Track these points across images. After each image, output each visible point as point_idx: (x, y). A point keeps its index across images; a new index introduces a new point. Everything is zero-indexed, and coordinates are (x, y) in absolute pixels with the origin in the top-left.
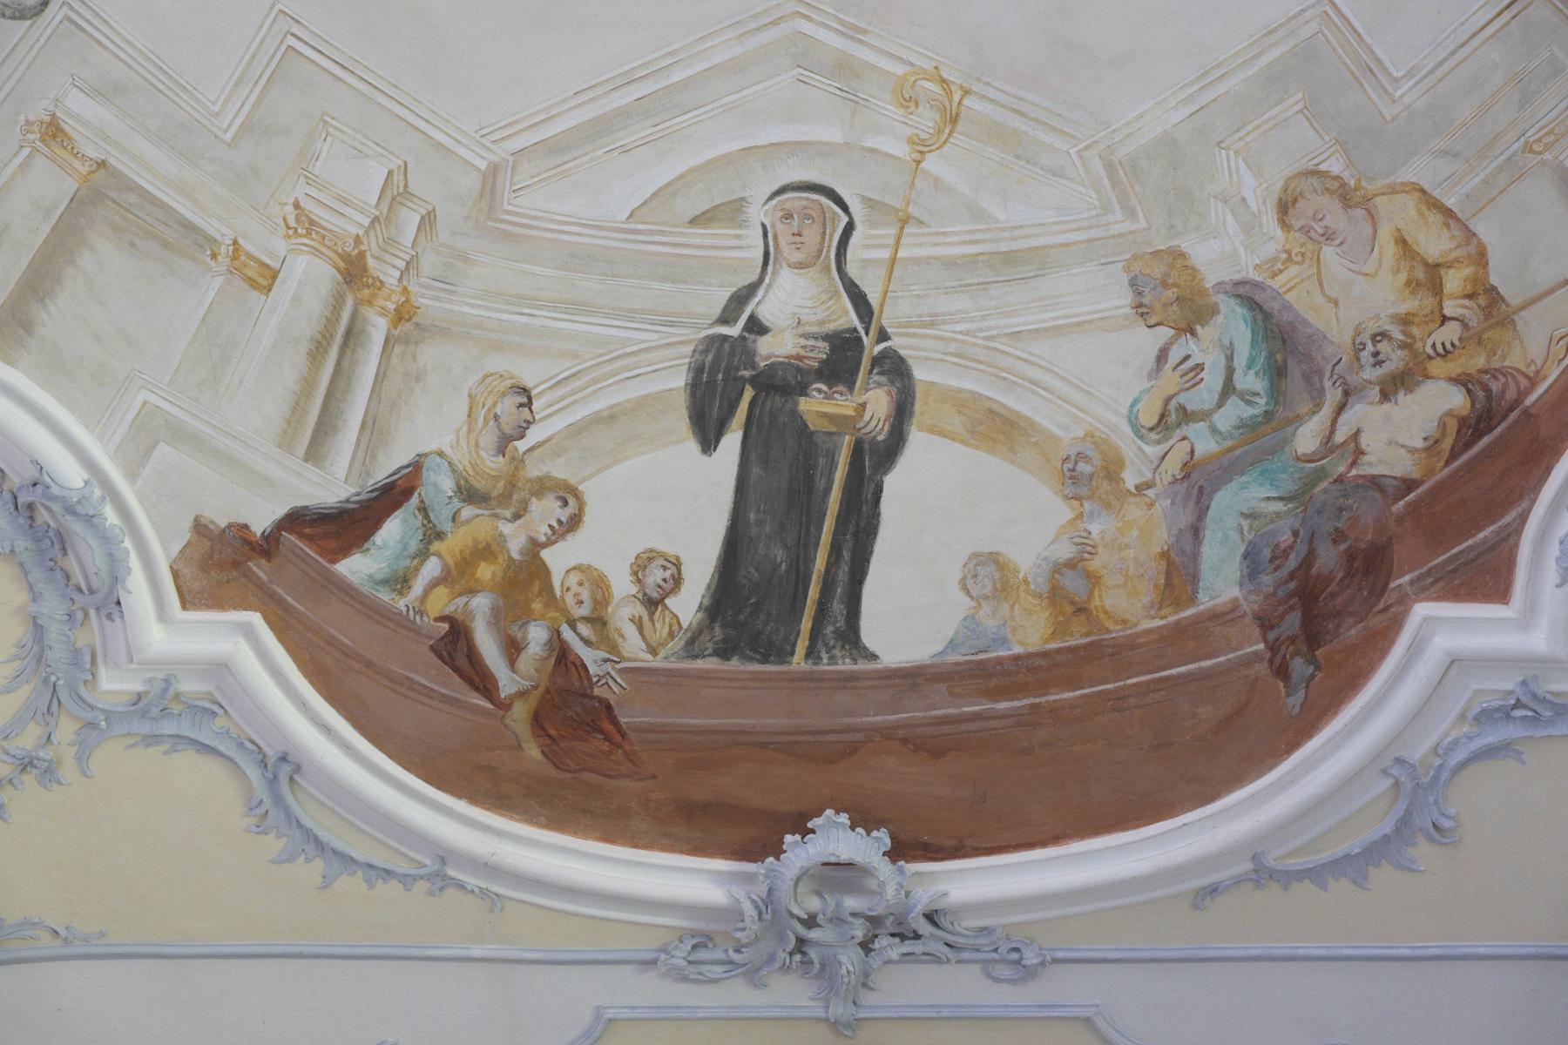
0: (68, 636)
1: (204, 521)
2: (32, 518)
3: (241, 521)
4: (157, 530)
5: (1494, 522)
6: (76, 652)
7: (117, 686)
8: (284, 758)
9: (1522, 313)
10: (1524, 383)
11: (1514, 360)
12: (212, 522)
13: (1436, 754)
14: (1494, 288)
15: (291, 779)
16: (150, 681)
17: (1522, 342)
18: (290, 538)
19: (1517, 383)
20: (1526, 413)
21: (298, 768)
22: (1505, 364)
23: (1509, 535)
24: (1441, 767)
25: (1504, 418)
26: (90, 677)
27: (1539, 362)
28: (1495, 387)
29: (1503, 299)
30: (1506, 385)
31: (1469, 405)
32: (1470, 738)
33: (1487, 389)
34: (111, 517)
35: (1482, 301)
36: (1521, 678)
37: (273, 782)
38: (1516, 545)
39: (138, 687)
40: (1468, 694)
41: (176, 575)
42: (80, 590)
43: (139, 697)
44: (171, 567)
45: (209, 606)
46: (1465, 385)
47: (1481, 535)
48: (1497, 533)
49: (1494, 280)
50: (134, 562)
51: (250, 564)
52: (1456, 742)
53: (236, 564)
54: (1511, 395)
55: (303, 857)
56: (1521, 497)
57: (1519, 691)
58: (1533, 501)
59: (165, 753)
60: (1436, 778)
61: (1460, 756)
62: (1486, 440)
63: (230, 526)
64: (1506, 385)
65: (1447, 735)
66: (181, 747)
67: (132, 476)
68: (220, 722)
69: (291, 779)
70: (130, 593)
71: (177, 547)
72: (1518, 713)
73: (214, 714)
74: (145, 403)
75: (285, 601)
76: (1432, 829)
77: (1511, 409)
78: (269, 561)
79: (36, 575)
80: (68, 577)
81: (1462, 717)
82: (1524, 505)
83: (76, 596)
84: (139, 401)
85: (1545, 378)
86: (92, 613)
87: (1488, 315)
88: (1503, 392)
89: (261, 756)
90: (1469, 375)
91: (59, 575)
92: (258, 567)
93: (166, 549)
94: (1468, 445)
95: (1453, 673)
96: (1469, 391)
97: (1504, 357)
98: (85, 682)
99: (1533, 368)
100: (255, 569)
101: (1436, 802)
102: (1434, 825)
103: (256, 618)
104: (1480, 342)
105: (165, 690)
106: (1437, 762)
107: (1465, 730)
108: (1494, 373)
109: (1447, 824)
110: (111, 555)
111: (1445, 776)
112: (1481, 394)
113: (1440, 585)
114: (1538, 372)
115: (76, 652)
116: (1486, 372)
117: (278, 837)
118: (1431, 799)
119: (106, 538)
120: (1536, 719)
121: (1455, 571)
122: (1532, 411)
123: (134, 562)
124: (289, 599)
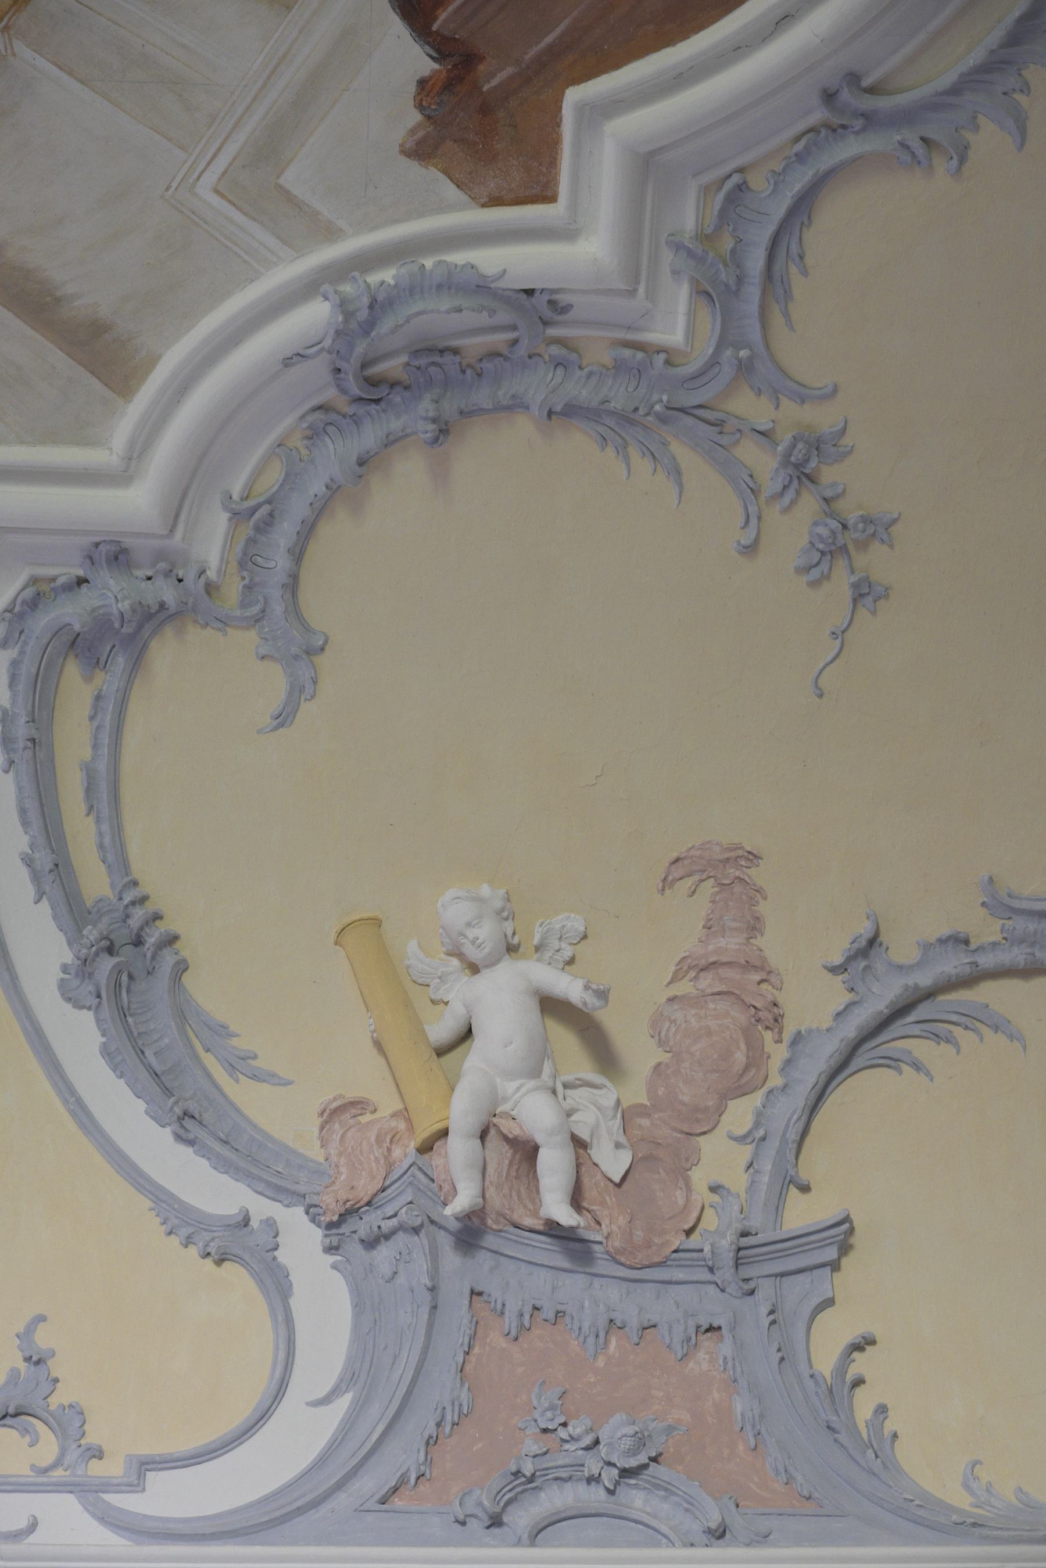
0: (590, 374)
1: (410, 144)
2: (393, 385)
3: (412, 88)
4: (420, 215)
6: (619, 367)
7: (681, 322)
8: (829, 97)
12: (413, 131)
15: (871, 90)
16: (675, 273)
18: (442, 19)
21: (853, 78)
26: (662, 356)
34: (388, 275)
37: (871, 120)
39: (683, 292)
41: (496, 201)
42: (515, 342)
43: (701, 293)
44: (483, 206)
45: (553, 163)
50: (458, 258)
51: (485, 88)
53: (485, 110)
55: (1018, 96)
59: (805, 273)
63: (420, 106)
66: (794, 248)
67: (331, 233)
68: (758, 182)
69: (871, 90)
70: (505, 271)
71: (450, 191)
73: (742, 188)
74: (217, 191)
75: (550, 47)
78: (481, 59)
79: (482, 397)
80: (495, 354)
83: (522, 351)
84: (215, 200)
86: (552, 332)
89: (823, 131)
91: (487, 365)
92: (492, 75)
93: (452, 208)
98: (668, 362)
100: (494, 82)
103: (574, 96)
105: (690, 253)
110: (440, 286)
115: (619, 367)
117: (977, 128)
119: (412, 289)
123: (458, 258)
124: (549, 39)
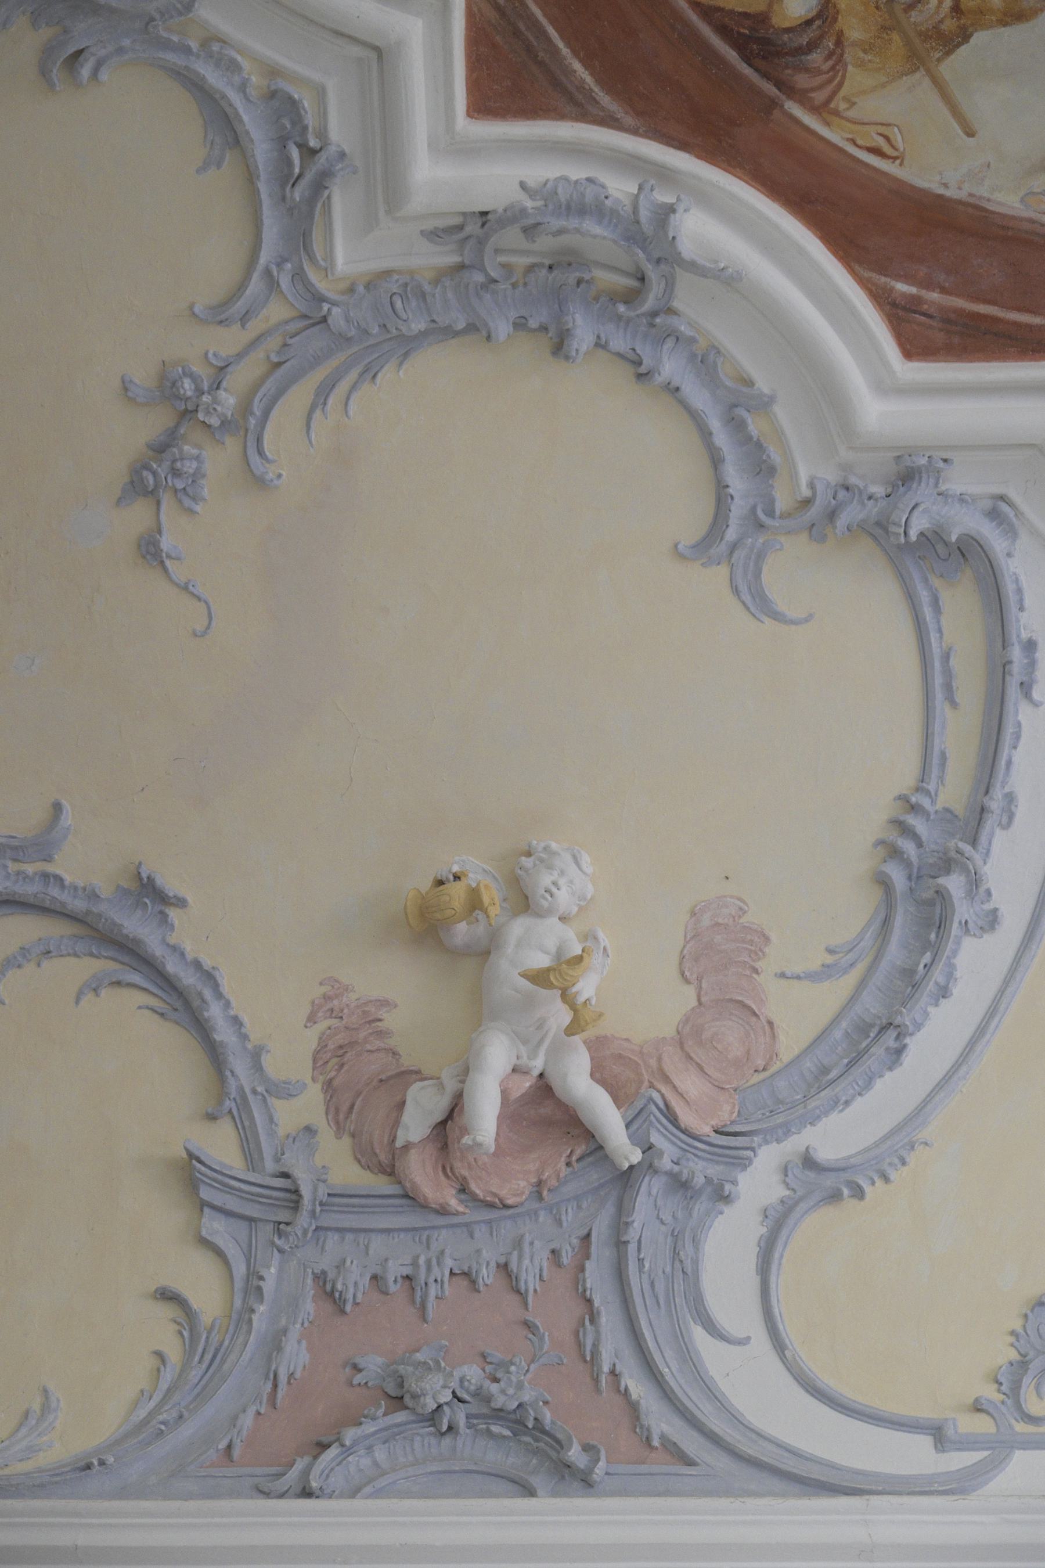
5: (599, 81)
9: (927, 82)
10: (819, 97)
11: (855, 78)
13: (205, 43)
14: (966, 38)
17: (883, 86)
19: (820, 87)
20: (773, 104)
22: (850, 68)
23: (577, 104)
24: (187, 51)
25: (766, 76)
27: (850, 114)
28: (815, 58)
29: (948, 53)
30: (819, 72)
31: (787, 24)
32: (243, 88)
33: (812, 46)
35: (949, 25)
36: (347, 150)
38: (562, 116)
40: (316, 76)
46: (819, 15)
47: (577, 66)
48: (581, 87)
49: (979, 38)
52: (234, 66)
54: (802, 81)
56: (639, 114)
57: (332, 149)
58: (634, 132)
60: (166, 45)
61: (213, 77)
62: (731, 55)
64: (819, 72)
65: (239, 52)
72: (295, 154)
76: (71, 49)
77: (779, 84)
81: (273, 72)
82: (629, 120)
85: (828, 124)
87: (925, 36)
88: (807, 70)
90: (835, 20)
94: (724, 31)
95: (356, 51)
96: (809, 23)
97: (861, 65)
99: (842, 106)
101: (120, 51)
102: (80, 52)
104: (884, 28)
106: (194, 45)
107: (254, 78)
108: (837, 56)
109: (85, 72)
111: (172, 58)
112: (804, 40)
113: (491, 14)
114: (836, 113)
116: (839, 43)
118: (126, 42)
120: (286, 179)
121: (517, 33)
122: (776, 114)
